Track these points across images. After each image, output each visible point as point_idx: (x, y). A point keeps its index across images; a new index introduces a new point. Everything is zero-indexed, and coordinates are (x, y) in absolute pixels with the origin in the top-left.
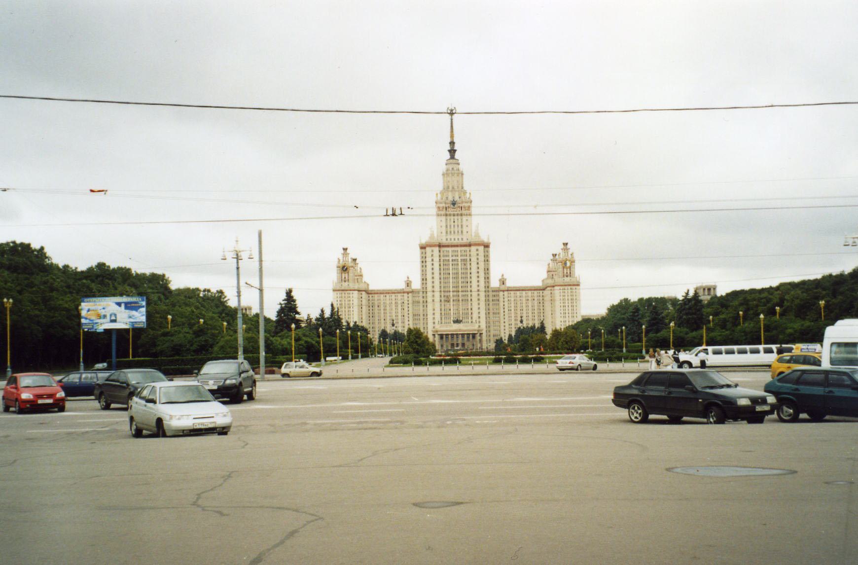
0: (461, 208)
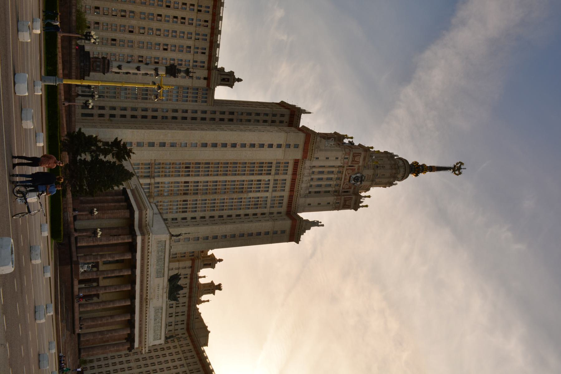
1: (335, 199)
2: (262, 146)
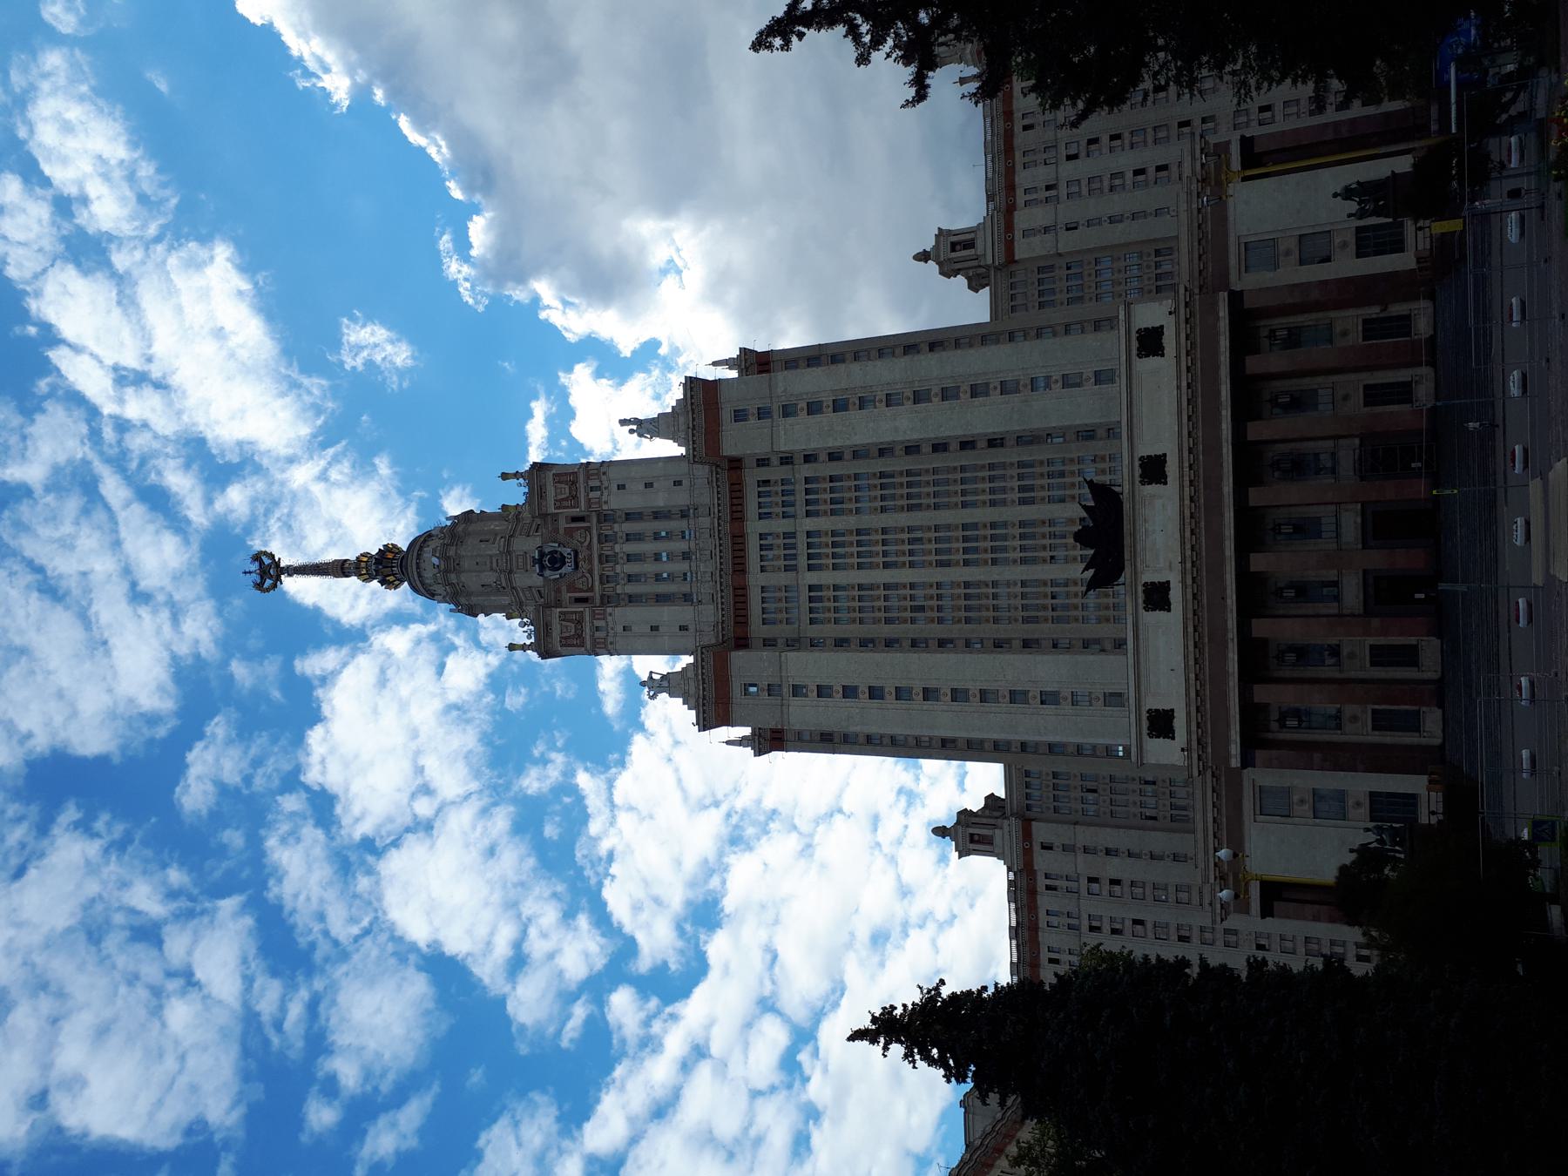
0: (575, 519)
1: (606, 502)
2: (849, 692)
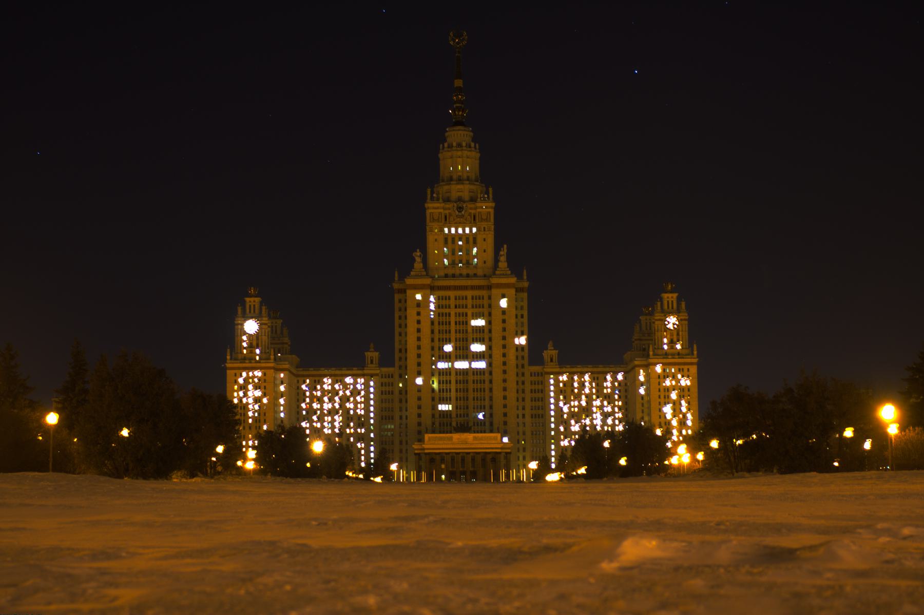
2: (419, 330)
